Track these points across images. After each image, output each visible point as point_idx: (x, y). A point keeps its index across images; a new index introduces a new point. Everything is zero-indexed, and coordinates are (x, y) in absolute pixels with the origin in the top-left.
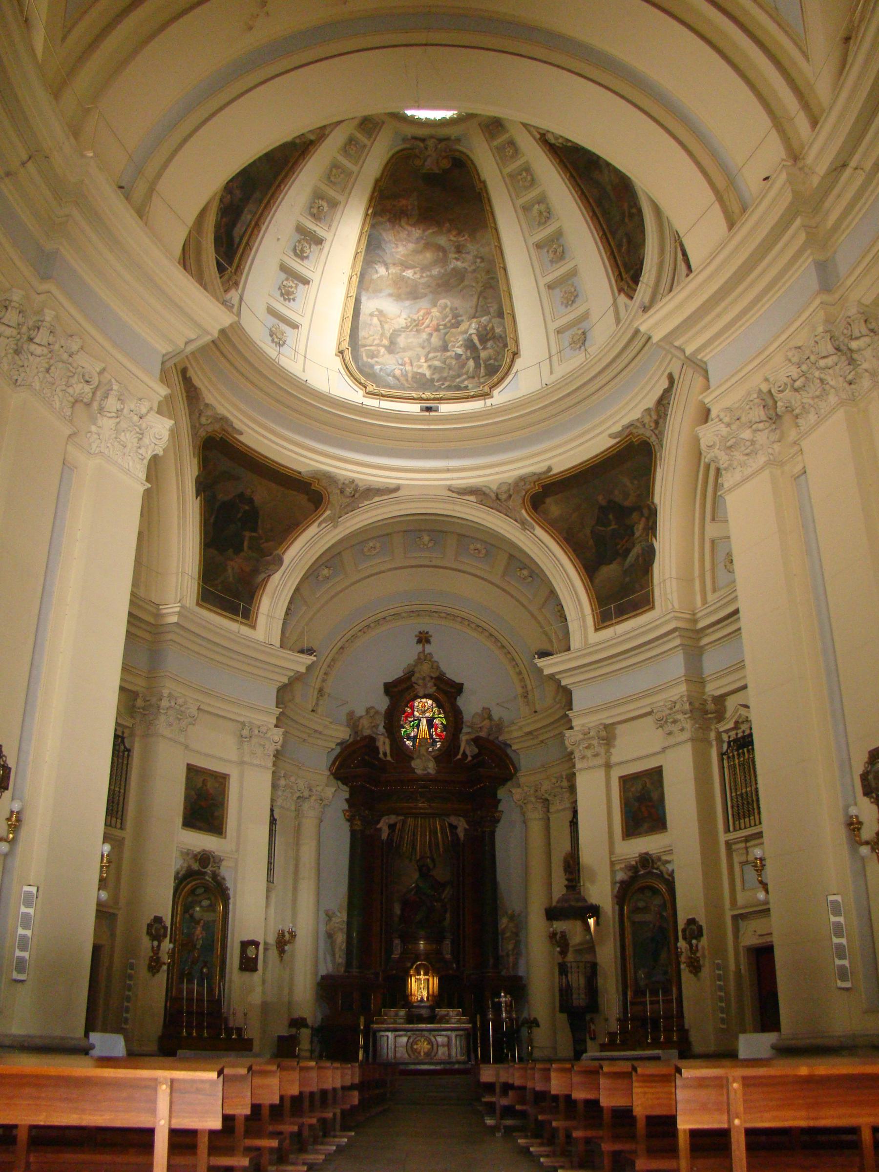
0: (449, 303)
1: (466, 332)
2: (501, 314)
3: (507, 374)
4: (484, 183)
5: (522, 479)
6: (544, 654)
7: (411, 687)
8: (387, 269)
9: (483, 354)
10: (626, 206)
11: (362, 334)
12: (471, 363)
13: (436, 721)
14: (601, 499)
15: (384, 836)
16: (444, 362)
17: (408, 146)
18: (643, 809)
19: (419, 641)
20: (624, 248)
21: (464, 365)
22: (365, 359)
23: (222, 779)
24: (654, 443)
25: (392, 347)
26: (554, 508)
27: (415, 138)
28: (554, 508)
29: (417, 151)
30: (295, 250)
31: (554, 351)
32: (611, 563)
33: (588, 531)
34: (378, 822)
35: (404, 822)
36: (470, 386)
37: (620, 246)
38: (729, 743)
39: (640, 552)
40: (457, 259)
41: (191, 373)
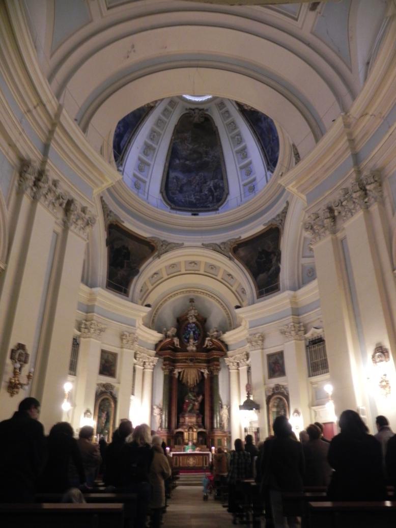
0: (203, 174)
1: (209, 185)
2: (222, 179)
3: (225, 201)
4: (216, 127)
5: (229, 241)
6: (237, 307)
7: (187, 319)
8: (179, 160)
9: (215, 194)
11: (170, 185)
12: (211, 197)
13: (196, 332)
14: (260, 249)
15: (177, 376)
16: (201, 196)
17: (187, 112)
19: (190, 302)
20: (270, 154)
21: (208, 198)
22: (171, 195)
23: (115, 355)
25: (181, 191)
26: (242, 252)
27: (191, 109)
28: (242, 252)
29: (191, 114)
30: (144, 152)
31: (242, 193)
32: (263, 273)
34: (174, 371)
35: (184, 371)
36: (210, 206)
37: (268, 152)
38: (309, 342)
40: (206, 157)
41: (104, 199)
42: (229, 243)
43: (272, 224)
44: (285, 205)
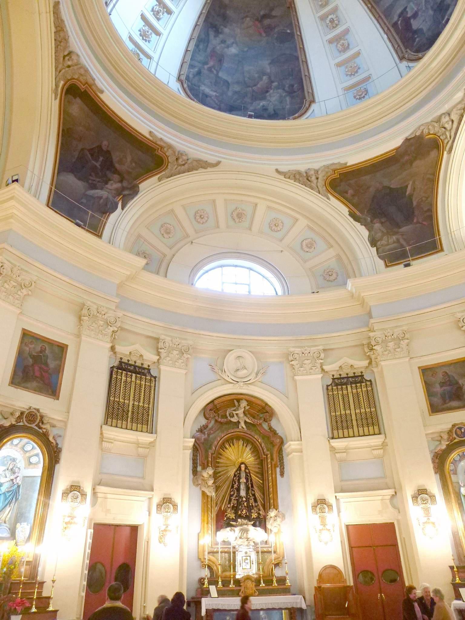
5: (87, 71)
10: (211, 64)
18: (37, 368)
24: (169, 167)
33: (80, 147)
39: (104, 197)
42: (82, 71)
43: (162, 147)
44: (211, 159)
